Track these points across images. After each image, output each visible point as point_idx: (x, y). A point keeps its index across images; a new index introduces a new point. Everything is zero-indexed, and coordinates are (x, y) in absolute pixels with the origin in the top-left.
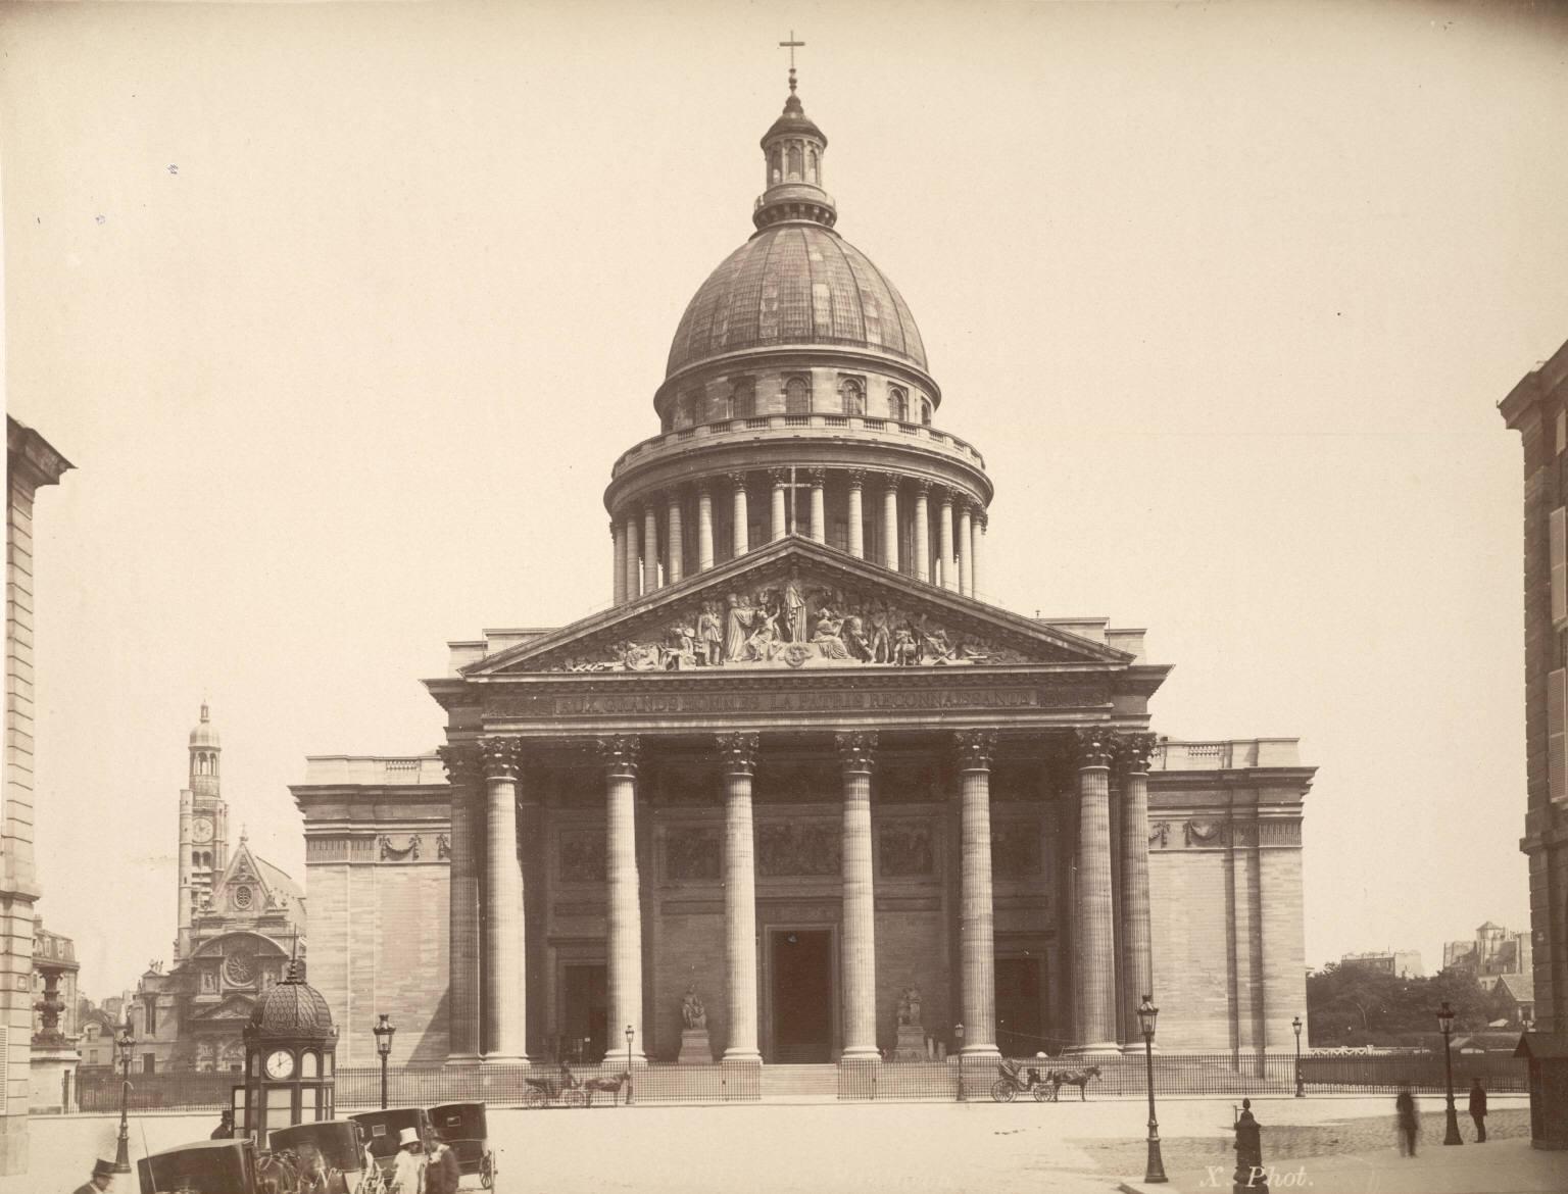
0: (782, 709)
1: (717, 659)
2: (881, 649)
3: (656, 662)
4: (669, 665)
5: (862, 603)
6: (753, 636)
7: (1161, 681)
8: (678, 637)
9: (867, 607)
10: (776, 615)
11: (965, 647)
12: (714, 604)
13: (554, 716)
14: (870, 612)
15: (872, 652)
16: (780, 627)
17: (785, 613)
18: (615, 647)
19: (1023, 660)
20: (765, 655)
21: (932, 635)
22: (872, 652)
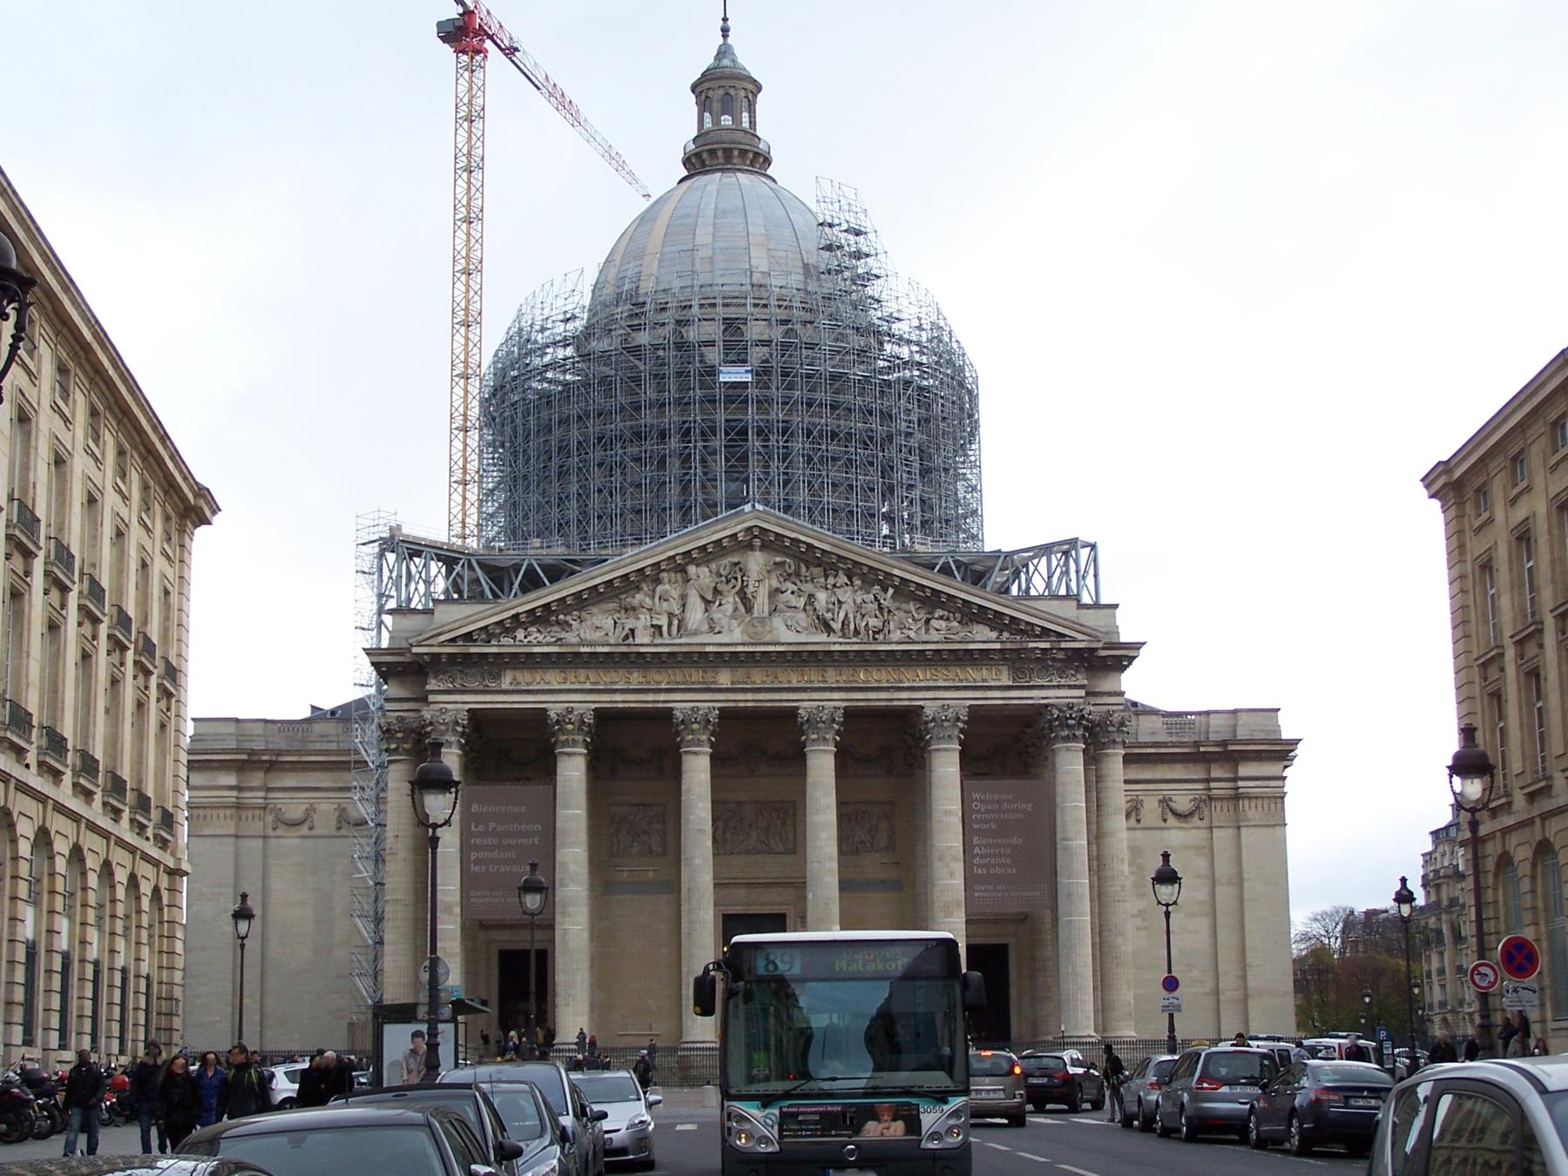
4: (627, 637)
5: (826, 577)
7: (1131, 659)
8: (634, 609)
9: (831, 580)
11: (934, 623)
13: (504, 687)
15: (836, 626)
18: (569, 618)
19: (994, 635)
22: (836, 626)
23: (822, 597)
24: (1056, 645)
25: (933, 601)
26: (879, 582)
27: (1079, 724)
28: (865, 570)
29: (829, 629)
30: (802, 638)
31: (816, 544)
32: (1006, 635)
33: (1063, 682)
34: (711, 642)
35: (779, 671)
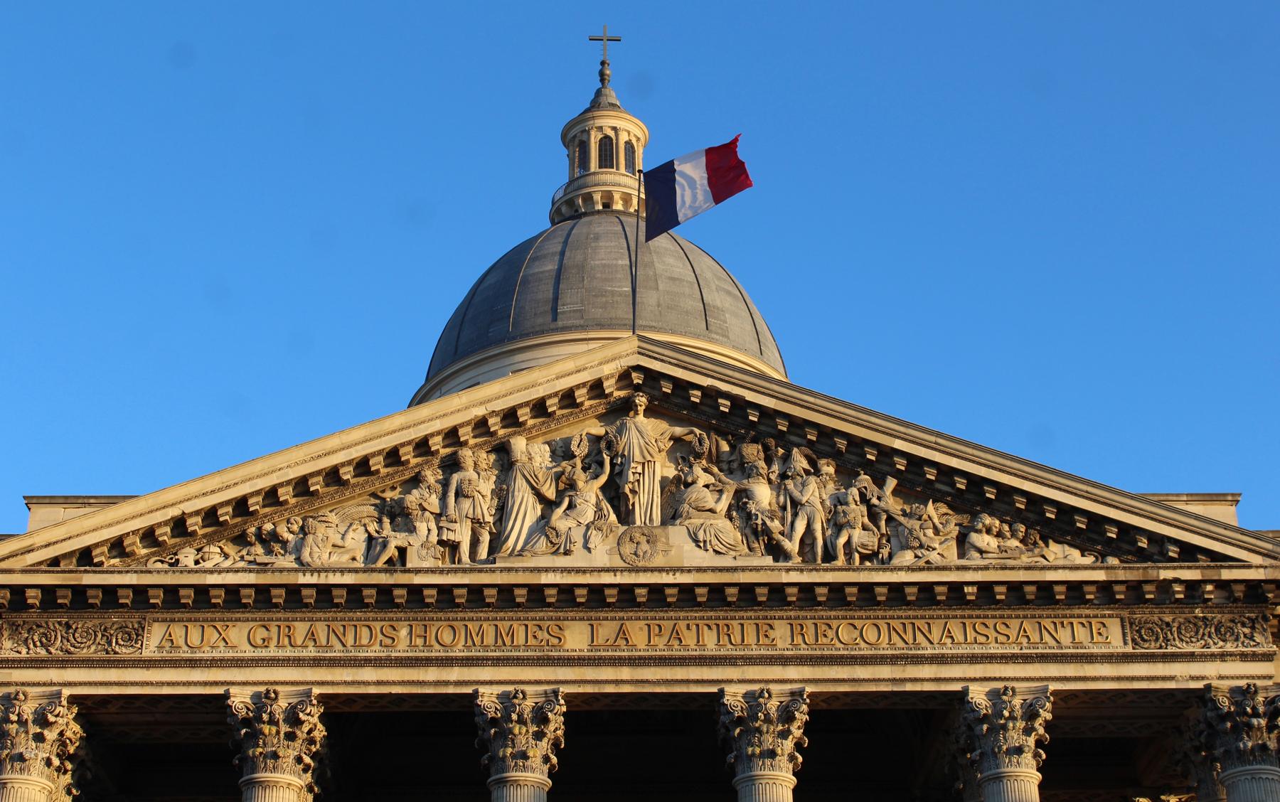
0: (615, 647)
1: (483, 552)
2: (808, 541)
3: (360, 558)
5: (769, 461)
6: (559, 511)
9: (775, 467)
10: (603, 479)
11: (975, 538)
12: (484, 455)
14: (783, 476)
15: (792, 546)
16: (611, 501)
17: (621, 473)
19: (1089, 560)
20: (580, 541)
21: (905, 514)
22: (792, 546)
23: (763, 494)
24: (1212, 575)
25: (972, 498)
26: (868, 467)
27: (1271, 728)
28: (842, 444)
29: (776, 551)
30: (726, 561)
31: (750, 396)
32: (1113, 561)
33: (1230, 647)
34: (547, 568)
35: (682, 625)
